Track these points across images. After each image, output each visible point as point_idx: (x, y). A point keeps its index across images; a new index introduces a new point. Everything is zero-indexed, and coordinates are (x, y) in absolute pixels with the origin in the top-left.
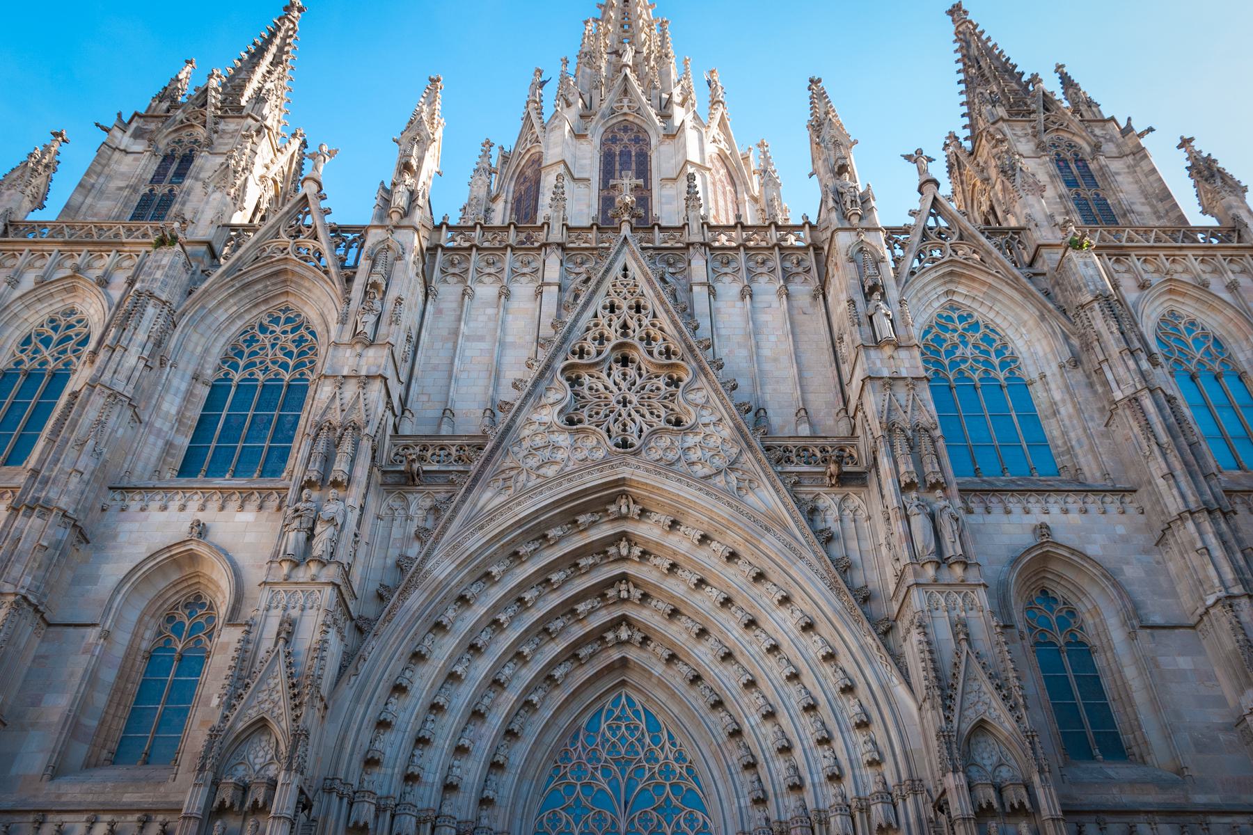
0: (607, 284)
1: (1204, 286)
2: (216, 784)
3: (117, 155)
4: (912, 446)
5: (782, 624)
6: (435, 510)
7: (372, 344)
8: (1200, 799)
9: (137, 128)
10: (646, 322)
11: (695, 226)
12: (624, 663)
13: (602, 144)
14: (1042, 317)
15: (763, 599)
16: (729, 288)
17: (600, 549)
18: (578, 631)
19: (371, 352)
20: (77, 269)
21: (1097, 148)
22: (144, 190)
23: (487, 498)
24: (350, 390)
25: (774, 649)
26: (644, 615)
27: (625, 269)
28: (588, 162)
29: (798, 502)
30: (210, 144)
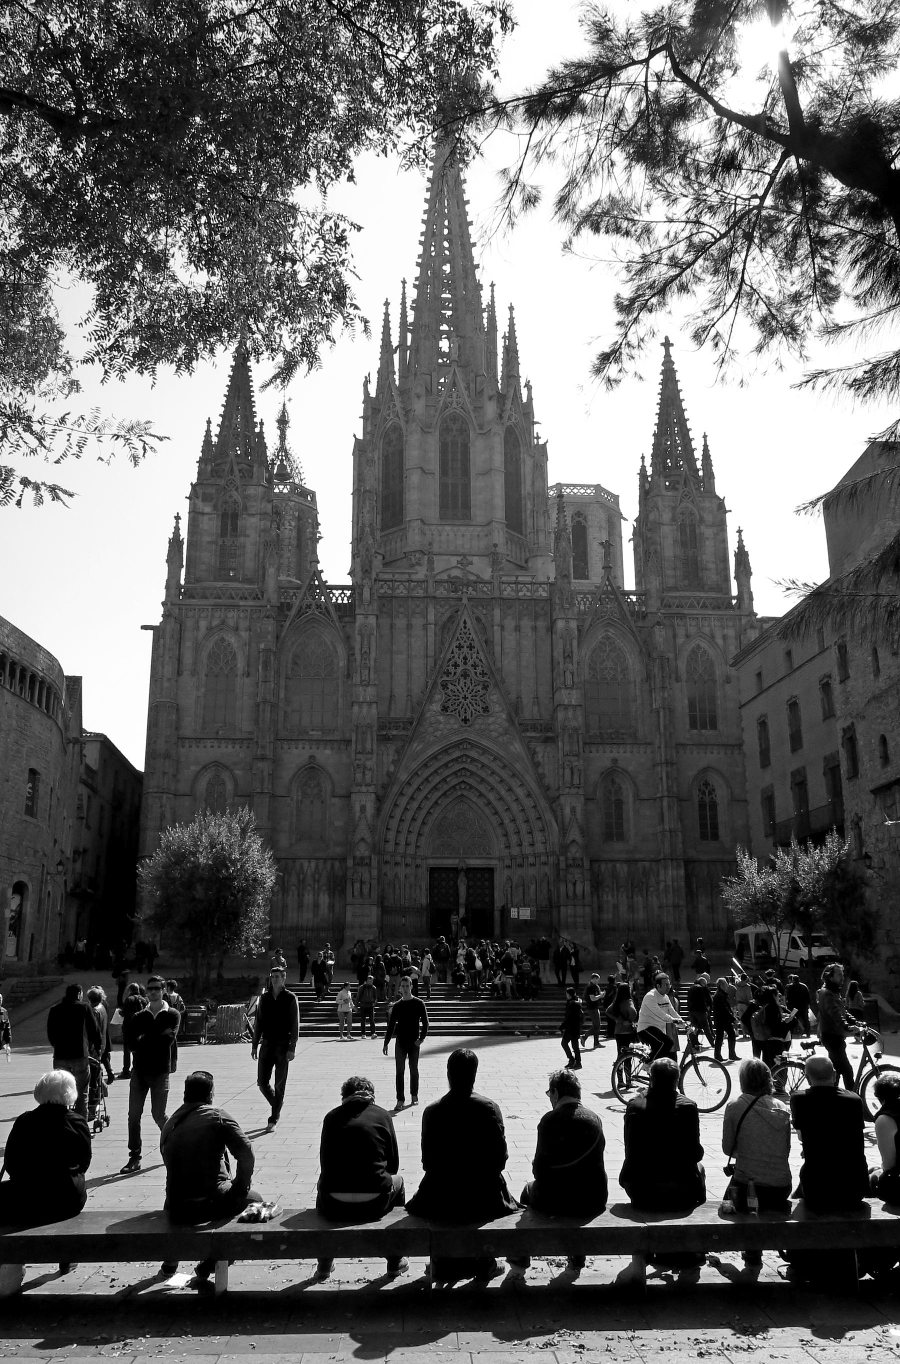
0: (458, 635)
1: (713, 637)
2: (354, 858)
3: (200, 517)
4: (570, 736)
5: (520, 792)
6: (397, 752)
7: (368, 685)
8: (638, 856)
9: (204, 493)
10: (474, 656)
11: (496, 584)
12: (462, 795)
13: (441, 435)
14: (641, 652)
15: (514, 783)
16: (510, 623)
17: (456, 760)
18: (446, 787)
19: (369, 689)
20: (223, 622)
21: (702, 520)
22: (220, 543)
23: (416, 746)
24: (365, 710)
25: (517, 800)
26: (471, 781)
27: (465, 622)
28: (432, 455)
29: (529, 749)
30: (245, 508)
